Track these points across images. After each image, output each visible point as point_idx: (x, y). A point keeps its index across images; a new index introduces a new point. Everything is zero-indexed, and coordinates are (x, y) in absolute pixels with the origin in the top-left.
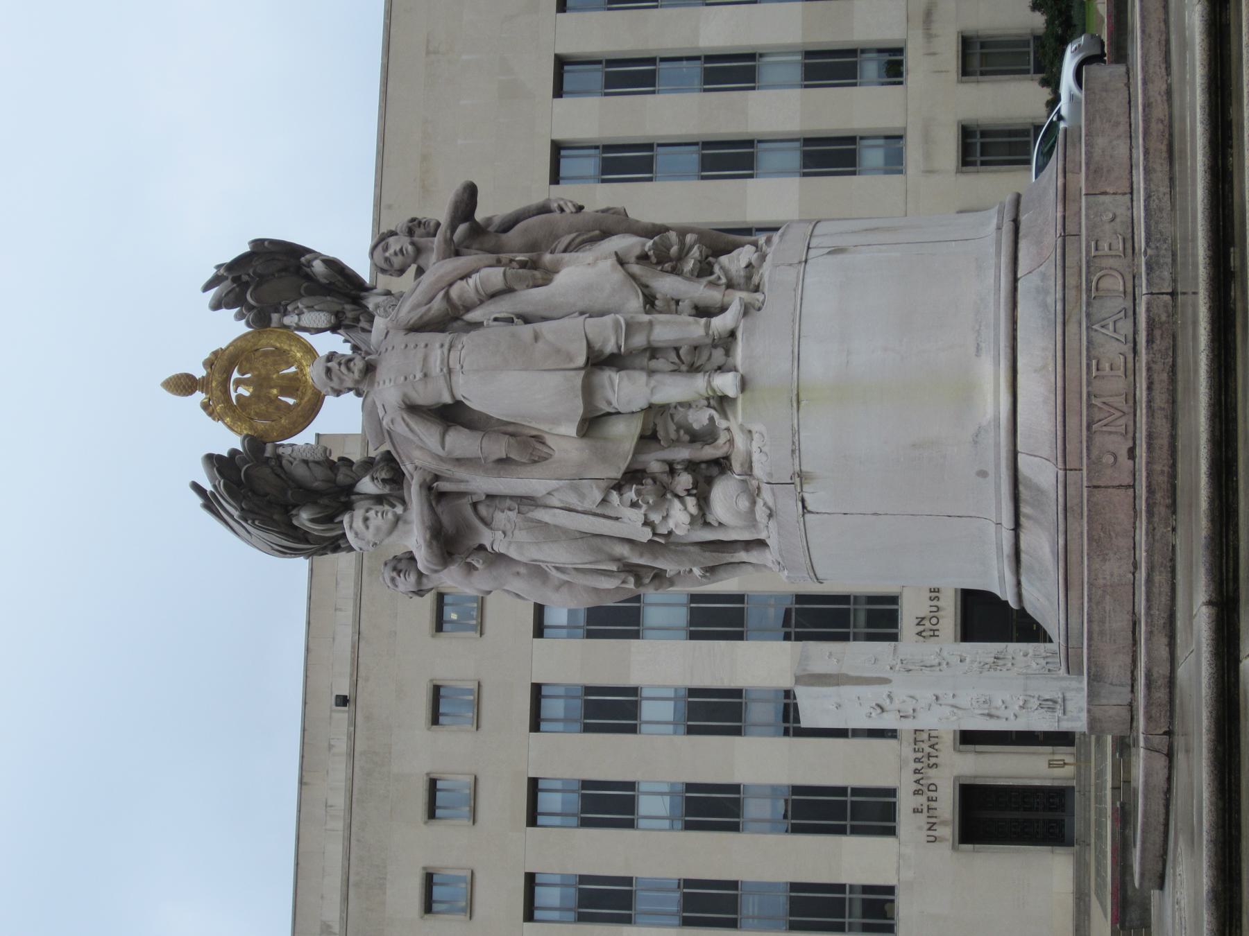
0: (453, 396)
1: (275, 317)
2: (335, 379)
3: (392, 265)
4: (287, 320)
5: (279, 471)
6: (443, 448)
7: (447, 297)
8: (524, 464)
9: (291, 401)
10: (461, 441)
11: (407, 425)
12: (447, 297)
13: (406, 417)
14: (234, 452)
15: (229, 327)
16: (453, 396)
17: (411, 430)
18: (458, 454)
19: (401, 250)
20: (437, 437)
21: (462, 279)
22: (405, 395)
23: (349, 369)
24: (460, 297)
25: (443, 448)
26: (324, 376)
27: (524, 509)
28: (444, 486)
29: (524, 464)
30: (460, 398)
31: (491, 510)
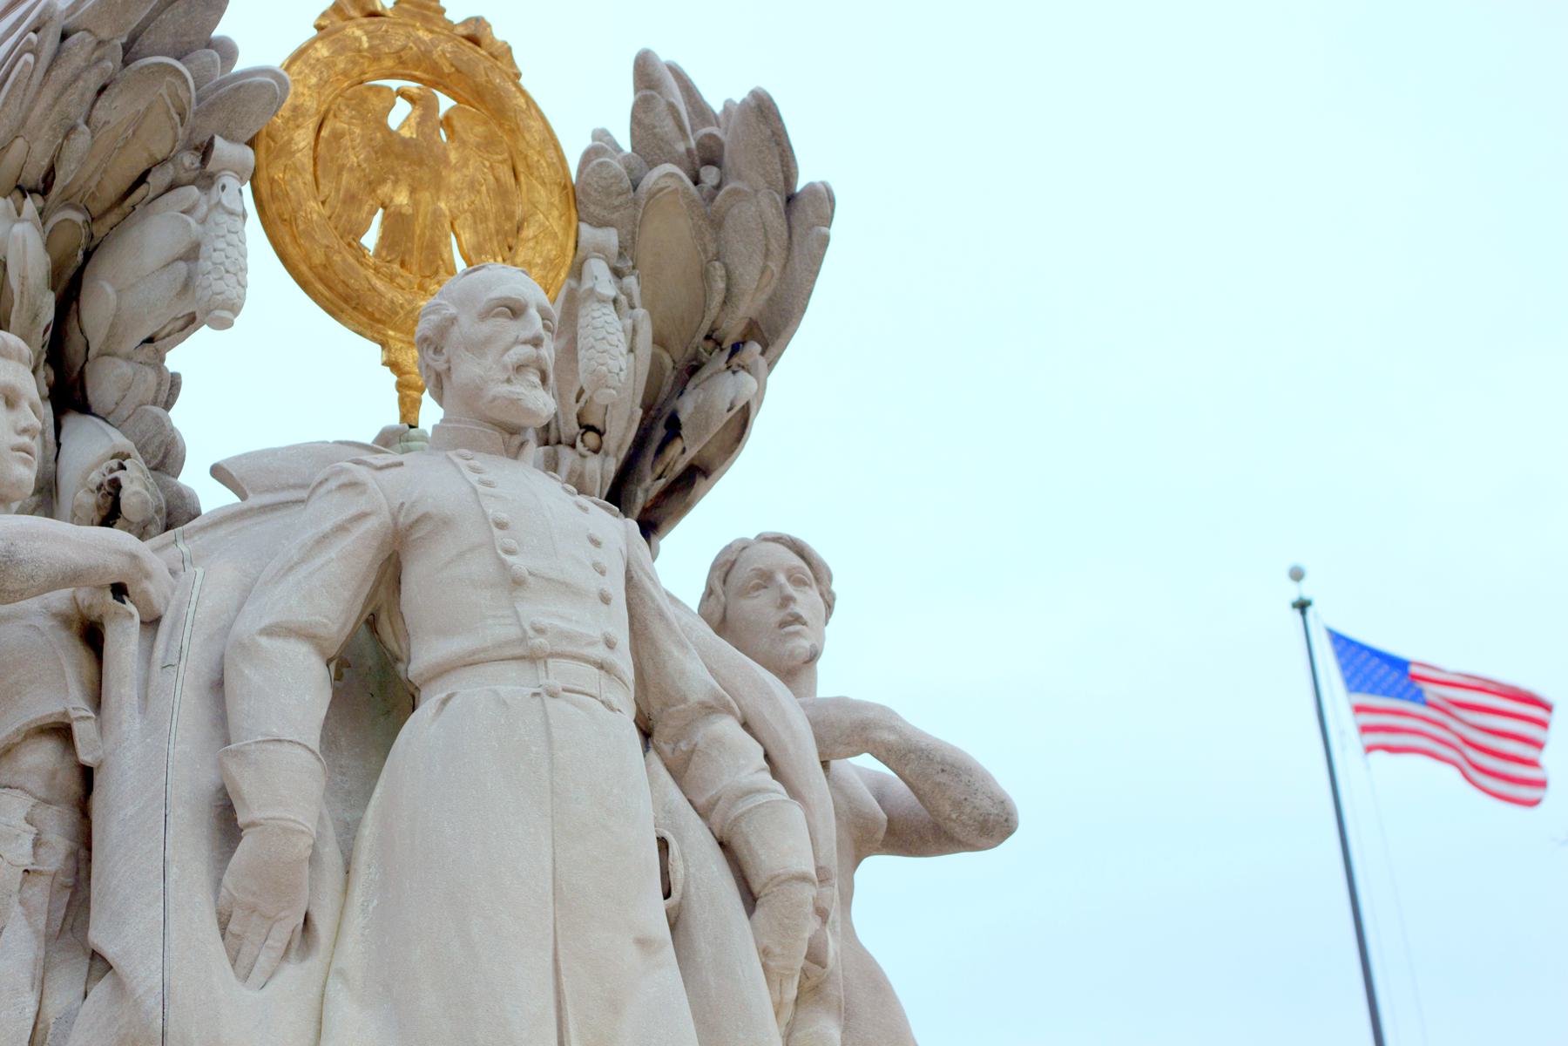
0: (443, 671)
1: (610, 238)
2: (487, 328)
3: (746, 591)
4: (599, 276)
5: (157, 180)
6: (269, 632)
7: (710, 709)
8: (218, 882)
9: (370, 239)
10: (293, 694)
11: (341, 529)
12: (710, 709)
13: (371, 524)
14: (227, 51)
15: (583, 108)
16: (443, 671)
17: (323, 540)
18: (247, 678)
19: (797, 619)
20: (303, 615)
21: (767, 757)
22: (447, 522)
23: (520, 368)
24: (718, 742)
25: (269, 632)
26: (497, 293)
27: (39, 894)
28: (123, 640)
29: (218, 882)
30: (426, 708)
31: (36, 784)
